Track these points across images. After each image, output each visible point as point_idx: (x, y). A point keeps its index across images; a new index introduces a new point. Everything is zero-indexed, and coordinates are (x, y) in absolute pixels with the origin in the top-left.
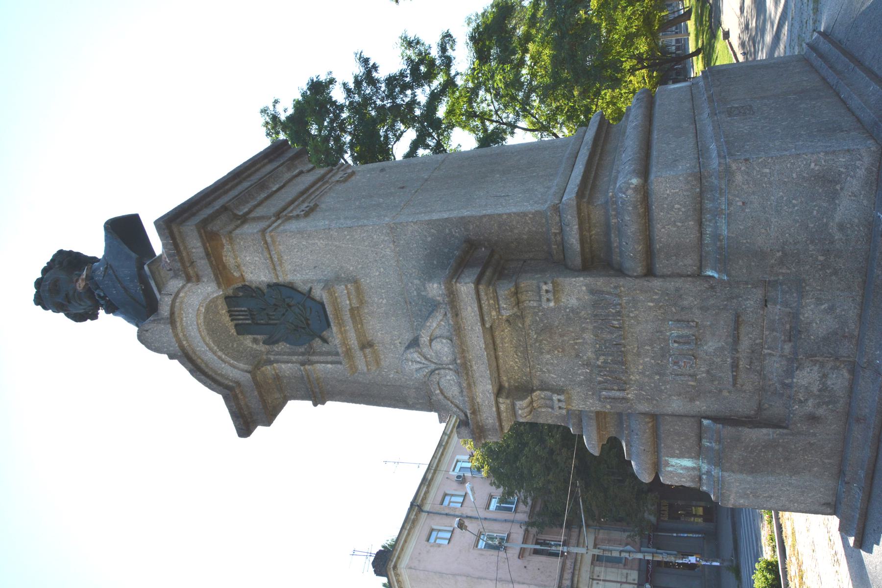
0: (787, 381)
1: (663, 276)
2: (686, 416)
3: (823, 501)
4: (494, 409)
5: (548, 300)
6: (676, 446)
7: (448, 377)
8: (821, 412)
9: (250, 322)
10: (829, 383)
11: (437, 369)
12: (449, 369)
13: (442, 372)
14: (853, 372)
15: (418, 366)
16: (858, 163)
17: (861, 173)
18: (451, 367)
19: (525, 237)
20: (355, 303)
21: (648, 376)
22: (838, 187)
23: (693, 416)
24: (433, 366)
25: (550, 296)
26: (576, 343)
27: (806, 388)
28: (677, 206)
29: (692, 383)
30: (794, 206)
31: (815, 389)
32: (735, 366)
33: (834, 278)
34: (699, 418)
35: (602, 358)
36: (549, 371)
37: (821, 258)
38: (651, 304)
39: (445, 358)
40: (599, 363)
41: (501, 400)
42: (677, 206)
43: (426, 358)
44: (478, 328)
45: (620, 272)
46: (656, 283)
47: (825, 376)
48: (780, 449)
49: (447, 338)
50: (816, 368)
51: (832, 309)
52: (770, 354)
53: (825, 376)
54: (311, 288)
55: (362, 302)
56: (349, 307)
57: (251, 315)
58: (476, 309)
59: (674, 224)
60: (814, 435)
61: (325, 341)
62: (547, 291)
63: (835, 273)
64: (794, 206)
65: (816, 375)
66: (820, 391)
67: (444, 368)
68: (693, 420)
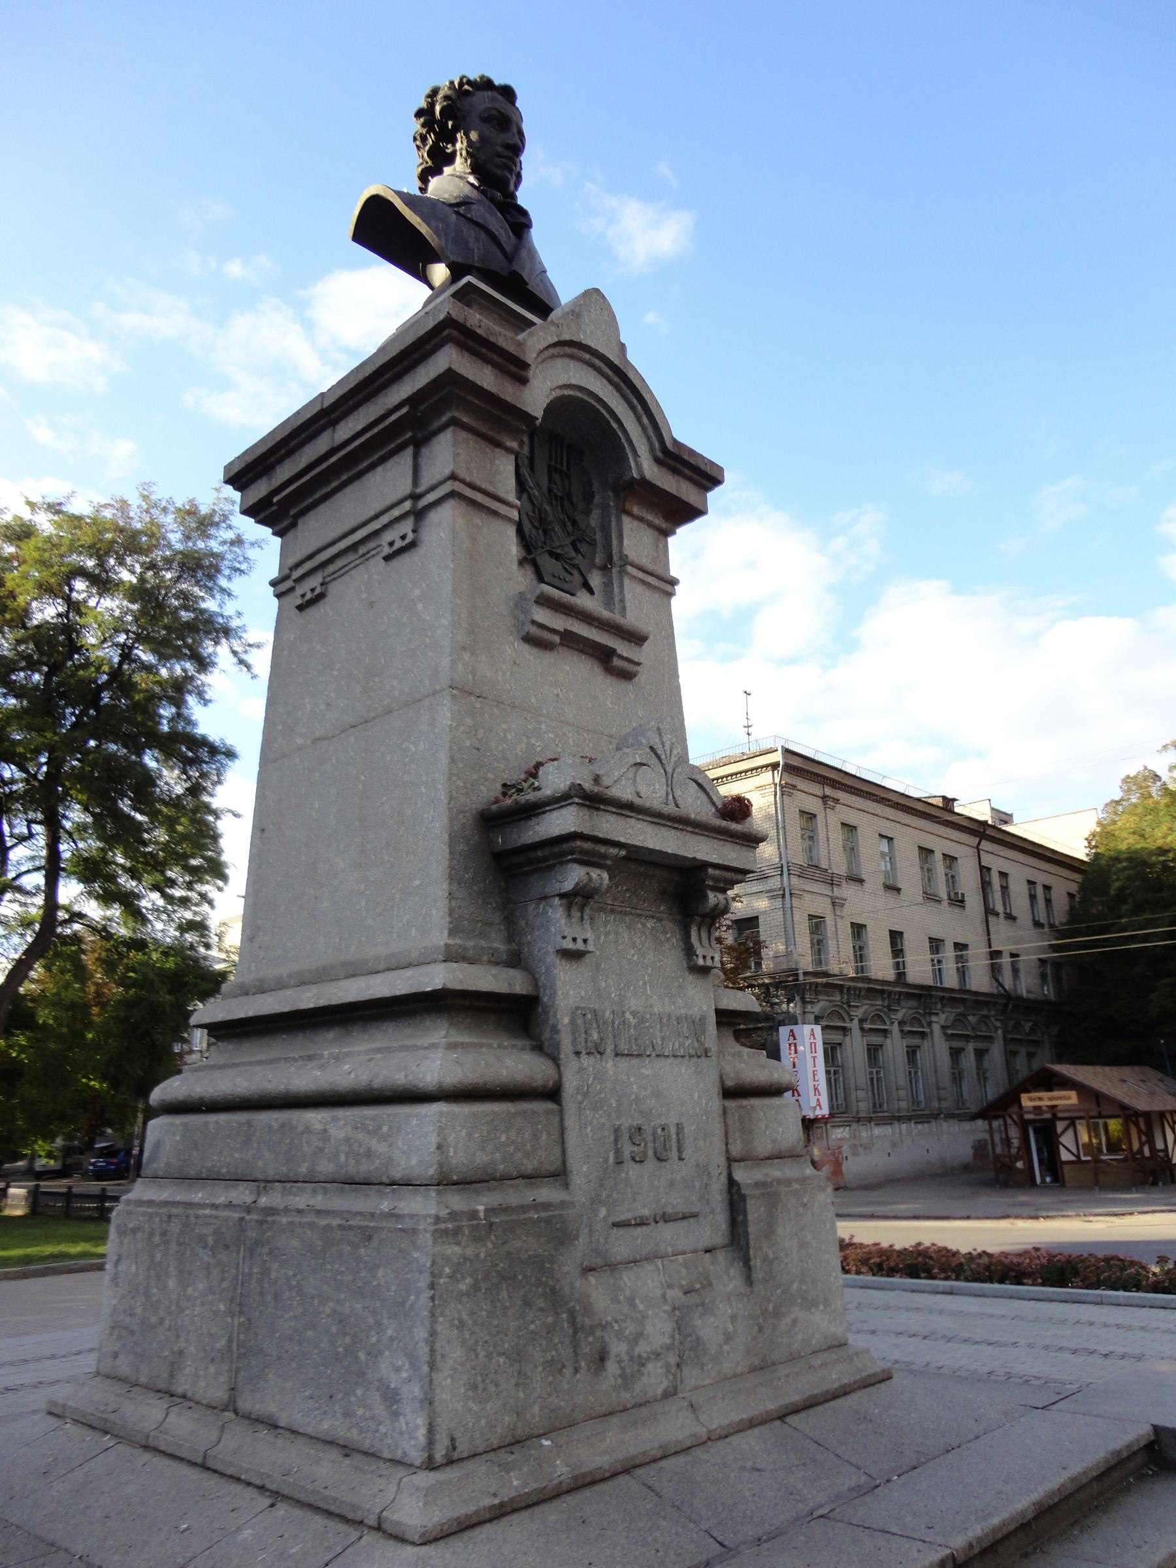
0: (637, 1301)
1: (725, 1112)
2: (564, 1152)
3: (457, 1434)
6: (513, 1134)
8: (612, 1367)
15: (667, 747)
20: (616, 662)
21: (615, 1089)
22: (822, 1307)
23: (564, 1162)
24: (669, 770)
26: (645, 984)
27: (642, 1334)
28: (781, 1130)
31: (642, 1348)
32: (642, 1223)
34: (560, 1175)
38: (696, 1096)
42: (781, 1130)
44: (714, 858)
46: (716, 1103)
56: (619, 652)
60: (576, 1371)
63: (760, 1330)
68: (559, 1162)
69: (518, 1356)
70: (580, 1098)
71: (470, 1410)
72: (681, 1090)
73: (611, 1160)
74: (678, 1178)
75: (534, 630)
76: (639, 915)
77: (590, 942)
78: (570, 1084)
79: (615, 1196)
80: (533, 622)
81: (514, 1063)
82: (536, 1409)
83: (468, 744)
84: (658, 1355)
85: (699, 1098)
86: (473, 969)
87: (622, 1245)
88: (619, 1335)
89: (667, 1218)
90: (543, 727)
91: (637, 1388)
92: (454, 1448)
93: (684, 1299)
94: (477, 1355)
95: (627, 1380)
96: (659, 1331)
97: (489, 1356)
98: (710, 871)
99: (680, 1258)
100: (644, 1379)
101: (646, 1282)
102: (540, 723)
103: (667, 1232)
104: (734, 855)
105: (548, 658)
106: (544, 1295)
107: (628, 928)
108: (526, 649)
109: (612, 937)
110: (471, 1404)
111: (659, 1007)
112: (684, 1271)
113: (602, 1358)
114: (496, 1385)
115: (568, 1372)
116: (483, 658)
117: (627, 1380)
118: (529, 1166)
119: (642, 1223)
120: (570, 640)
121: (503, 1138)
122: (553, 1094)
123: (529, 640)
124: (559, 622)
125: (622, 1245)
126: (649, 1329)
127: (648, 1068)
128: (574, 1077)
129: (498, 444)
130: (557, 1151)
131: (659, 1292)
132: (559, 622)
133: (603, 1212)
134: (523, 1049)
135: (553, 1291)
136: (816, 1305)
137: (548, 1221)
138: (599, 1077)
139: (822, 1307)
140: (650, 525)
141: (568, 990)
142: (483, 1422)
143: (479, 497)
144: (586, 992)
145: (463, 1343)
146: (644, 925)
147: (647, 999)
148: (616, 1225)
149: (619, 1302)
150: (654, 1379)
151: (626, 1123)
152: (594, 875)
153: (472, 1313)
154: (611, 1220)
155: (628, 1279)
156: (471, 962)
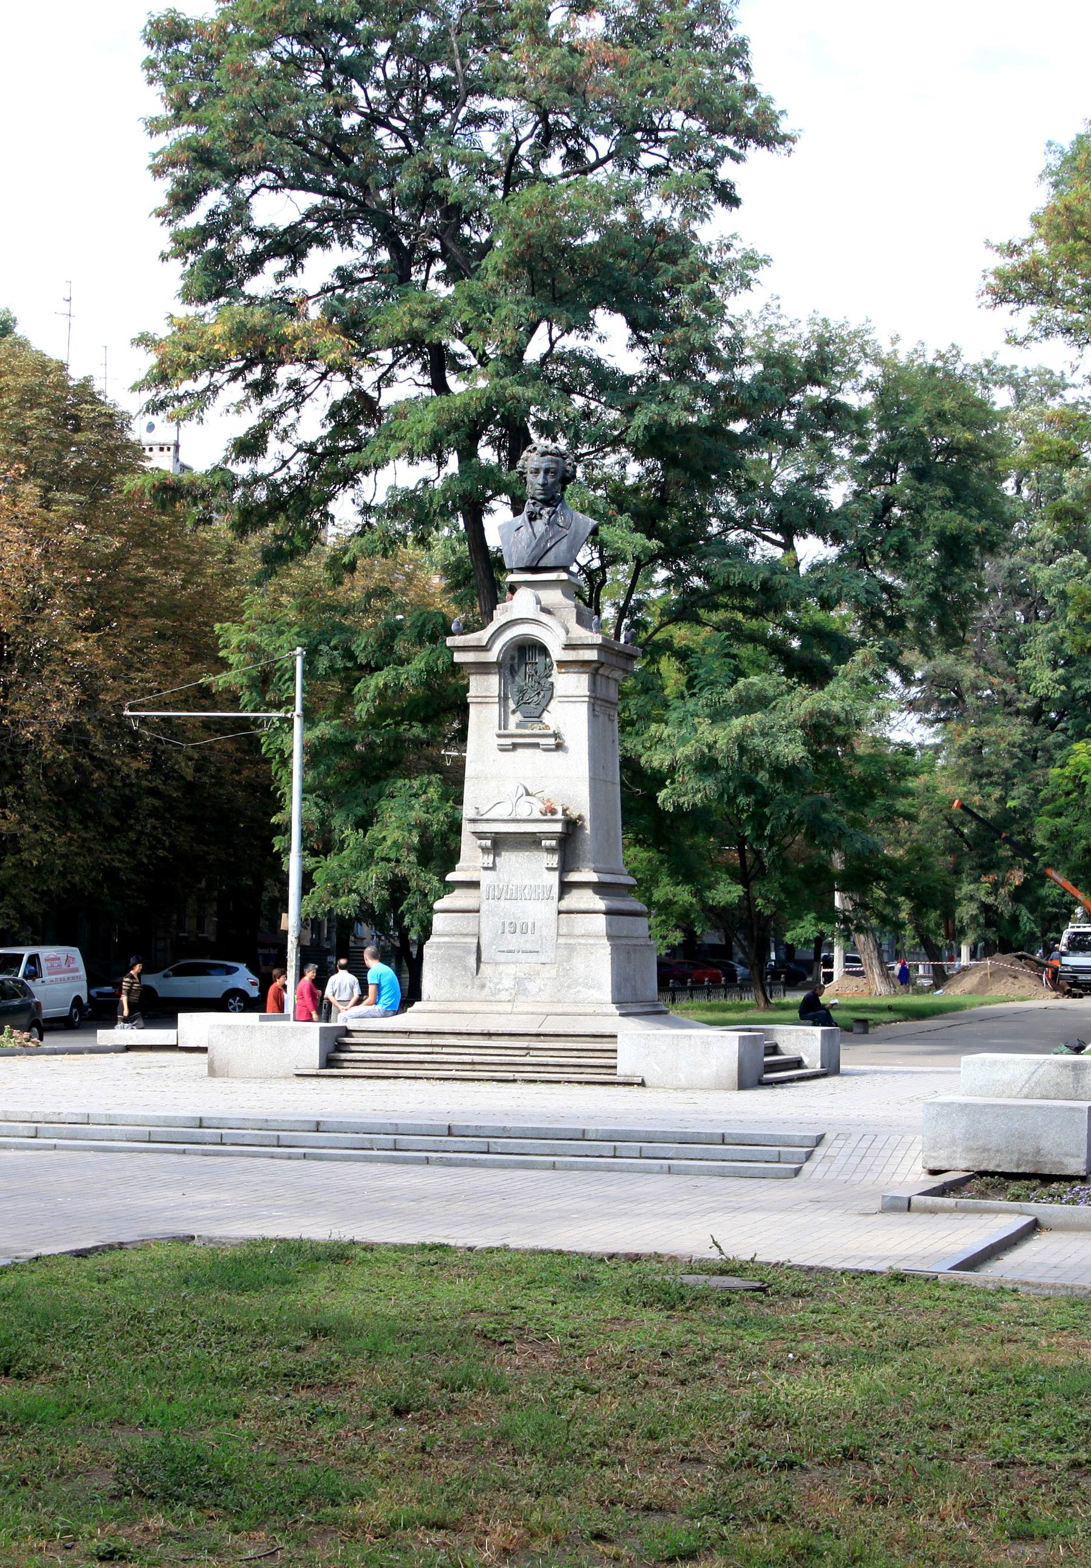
31: (500, 986)
45: (560, 898)
55: (545, 750)
69: (451, 980)
78: (483, 909)
87: (502, 957)
95: (493, 994)
96: (507, 983)
101: (511, 969)
111: (526, 882)
113: (483, 986)
120: (515, 746)
124: (509, 741)
127: (519, 903)
132: (509, 741)
150: (504, 996)
151: (508, 921)
155: (501, 968)
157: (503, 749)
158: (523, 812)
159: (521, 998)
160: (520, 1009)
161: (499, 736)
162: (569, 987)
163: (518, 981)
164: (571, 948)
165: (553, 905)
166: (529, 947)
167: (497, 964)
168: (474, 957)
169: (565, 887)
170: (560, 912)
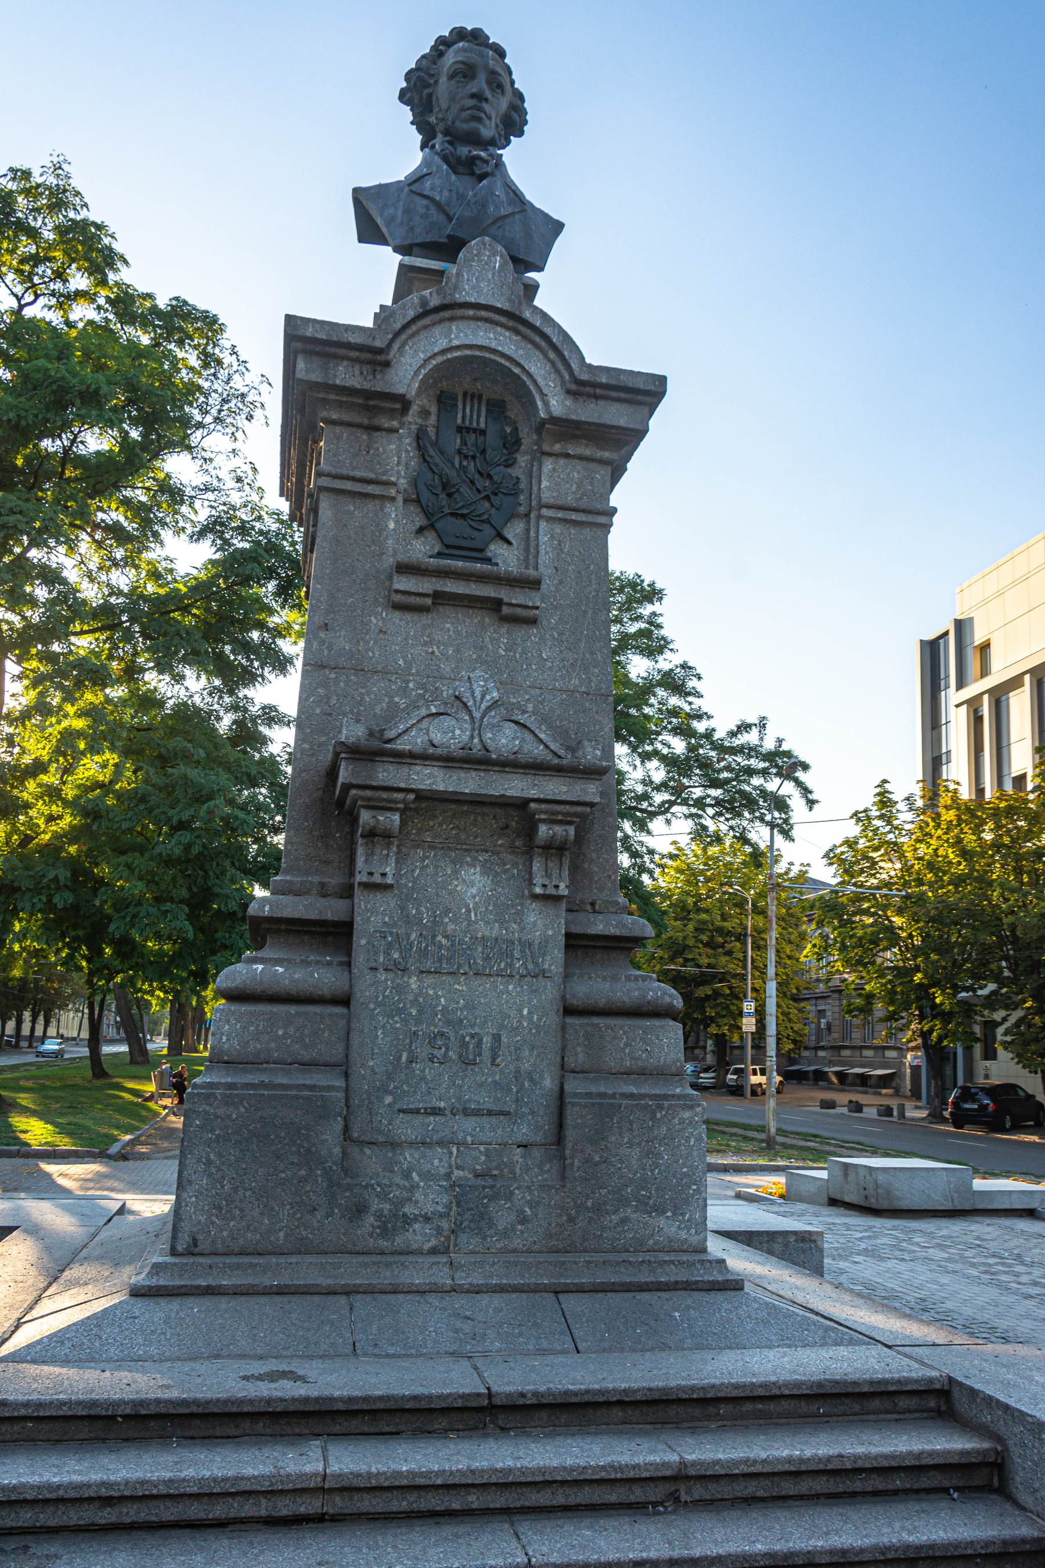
0: (414, 1174)
1: (563, 1028)
2: (347, 1047)
3: (200, 1237)
4: (402, 785)
5: (544, 886)
6: (291, 1030)
7: (458, 732)
9: (459, 421)
10: (417, 1226)
11: (472, 718)
12: (472, 737)
13: (467, 726)
14: (433, 1251)
16: (693, 1231)
17: (683, 1235)
18: (476, 741)
19: (586, 866)
20: (505, 610)
21: (416, 1000)
24: (477, 715)
25: (551, 891)
26: (469, 911)
27: (410, 1200)
29: (404, 1059)
30: (652, 1171)
31: (408, 1209)
32: (435, 1112)
33: (565, 1218)
34: (344, 1067)
35: (444, 941)
36: (424, 868)
37: (589, 1203)
38: (525, 1012)
39: (490, 735)
40: (439, 938)
41: (411, 796)
43: (489, 708)
44: (533, 793)
45: (567, 976)
46: (553, 1019)
47: (427, 1219)
48: (303, 1172)
49: (521, 747)
50: (440, 1208)
51: (524, 1221)
52: (451, 1153)
53: (427, 1219)
54: (509, 543)
56: (506, 600)
57: (475, 430)
58: (564, 798)
59: (626, 1045)
61: (420, 531)
62: (557, 887)
63: (571, 1220)
64: (652, 1171)
65: (429, 1208)
66: (404, 1215)
67: (473, 730)
68: (341, 1056)
70: (372, 1006)
71: (213, 1223)
72: (517, 1008)
73: (404, 1059)
74: (490, 1080)
75: (397, 598)
76: (466, 850)
77: (390, 876)
79: (405, 1088)
80: (397, 591)
81: (318, 974)
82: (281, 1234)
83: (318, 711)
84: (429, 1219)
85: (529, 1013)
86: (306, 900)
87: (407, 1129)
88: (384, 1196)
89: (467, 1112)
90: (411, 685)
91: (399, 1240)
92: (196, 1245)
93: (473, 1181)
94: (223, 1187)
96: (430, 1199)
97: (235, 1189)
98: (532, 805)
99: (482, 1148)
100: (409, 1235)
102: (408, 682)
103: (469, 1124)
104: (564, 789)
105: (426, 619)
106: (298, 1153)
107: (453, 862)
108: (397, 615)
109: (430, 870)
110: (215, 1219)
111: (482, 930)
112: (483, 1158)
113: (360, 1210)
114: (242, 1210)
115: (319, 1215)
116: (343, 633)
117: (386, 1232)
118: (305, 1055)
119: (435, 1112)
120: (439, 598)
121: (280, 1032)
122: (344, 1001)
123: (398, 607)
124: (427, 586)
125: (407, 1129)
126: (418, 1196)
128: (371, 986)
129: (378, 429)
130: (340, 1047)
131: (442, 1171)
132: (427, 586)
133: (388, 1099)
134: (329, 964)
135: (308, 1151)
136: (664, 1212)
137: (308, 1098)
138: (400, 989)
139: (669, 1214)
140: (581, 458)
141: (372, 915)
142: (225, 1234)
143: (349, 486)
144: (391, 917)
145: (210, 1175)
146: (475, 859)
147: (469, 925)
148: (400, 1111)
149: (392, 1171)
150: (420, 1235)
152: (381, 818)
153: (220, 1155)
154: (397, 1106)
155: (409, 1156)
156: (297, 894)
157: (405, 606)
158: (505, 740)
159: (468, 1241)
160: (477, 1279)
161: (405, 569)
162: (599, 1209)
163: (461, 1195)
164: (606, 1108)
165: (549, 992)
166: (485, 1100)
167: (394, 1145)
168: (338, 1125)
169: (578, 944)
170: (569, 1011)
